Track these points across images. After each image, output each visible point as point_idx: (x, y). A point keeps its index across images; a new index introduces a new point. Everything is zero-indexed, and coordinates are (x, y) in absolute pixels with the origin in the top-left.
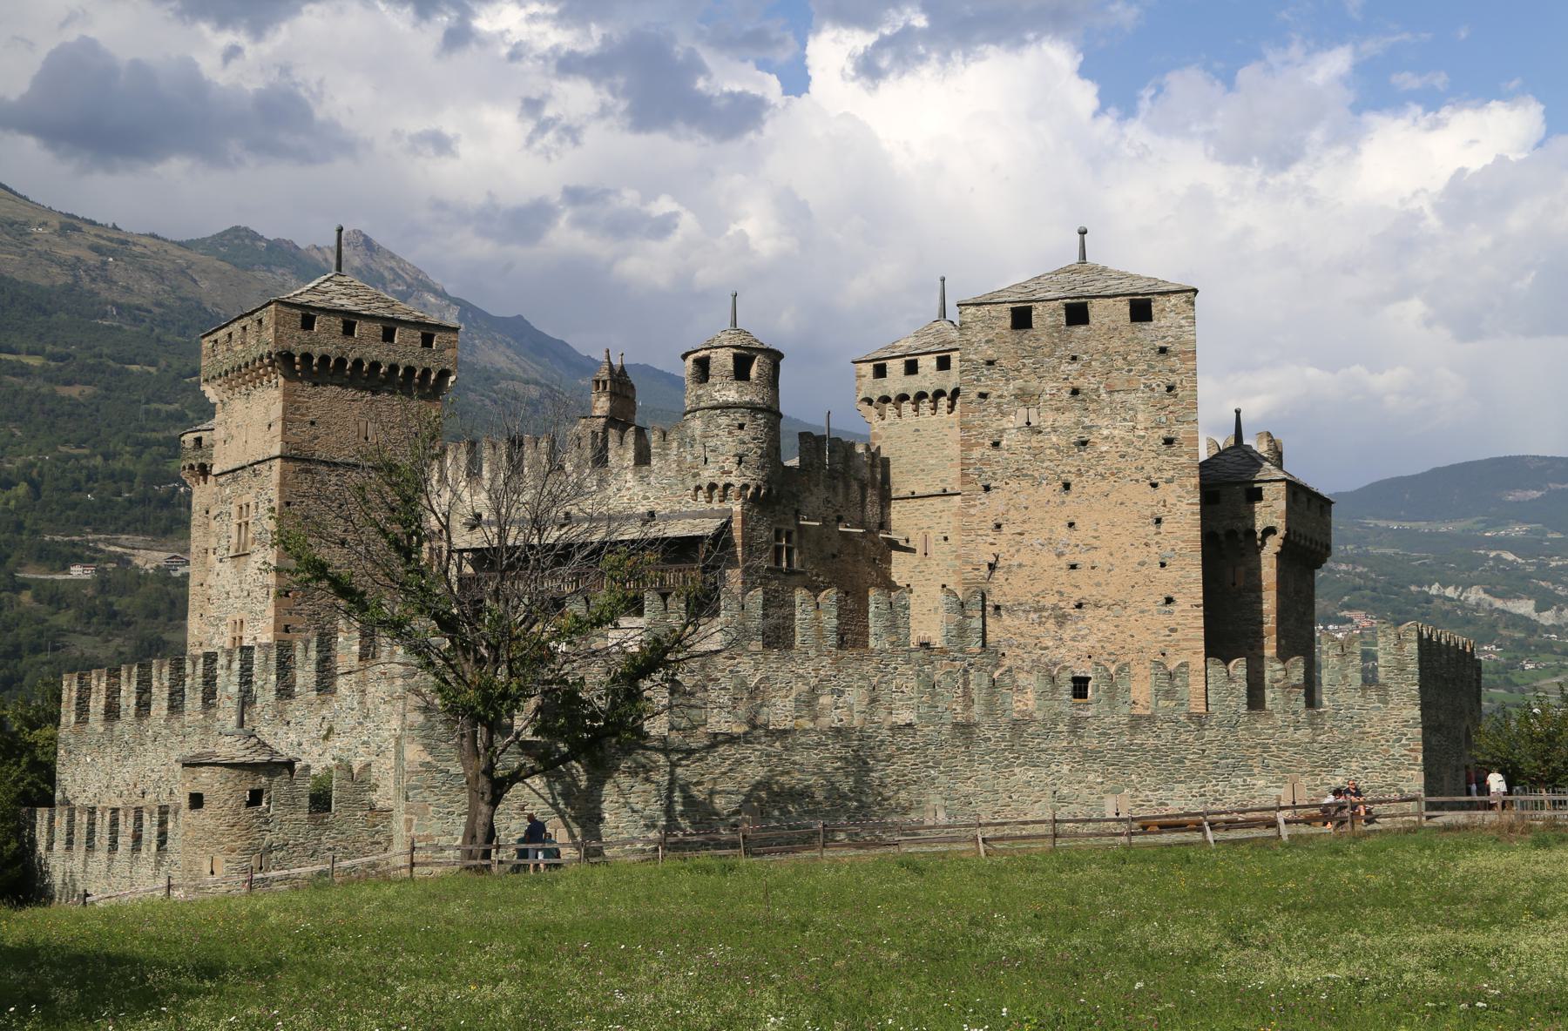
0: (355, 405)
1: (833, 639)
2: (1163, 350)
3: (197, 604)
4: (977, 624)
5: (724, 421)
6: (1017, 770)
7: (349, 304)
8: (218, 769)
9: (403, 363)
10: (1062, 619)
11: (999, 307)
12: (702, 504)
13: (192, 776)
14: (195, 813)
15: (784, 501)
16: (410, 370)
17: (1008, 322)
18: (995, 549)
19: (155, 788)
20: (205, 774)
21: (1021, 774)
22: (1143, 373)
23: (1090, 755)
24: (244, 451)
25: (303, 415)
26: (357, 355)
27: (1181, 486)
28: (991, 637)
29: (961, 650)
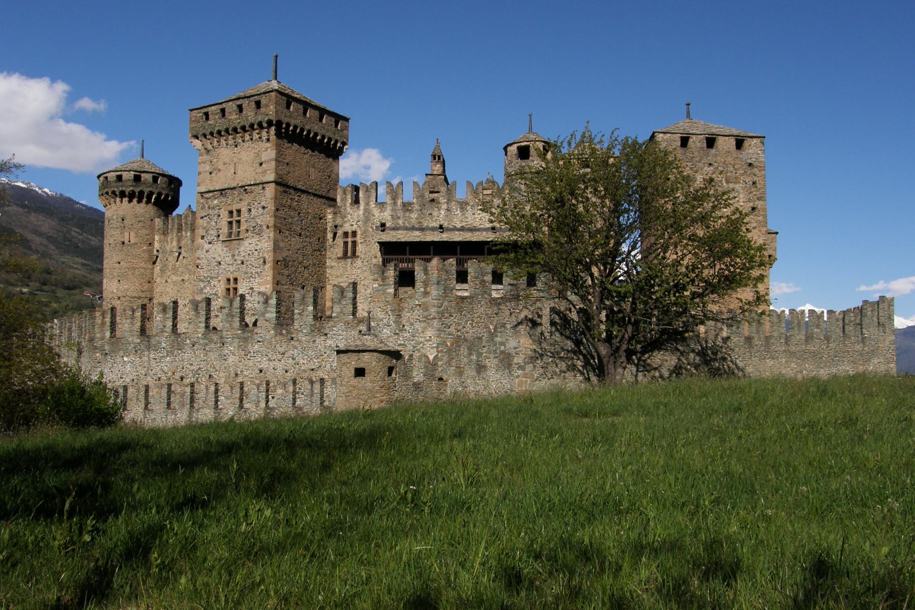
0: (305, 156)
2: (750, 165)
3: (115, 274)
6: (767, 361)
8: (375, 354)
9: (328, 134)
11: (675, 136)
13: (357, 358)
14: (359, 379)
17: (679, 144)
19: (194, 375)
20: (366, 356)
22: (742, 175)
24: (234, 179)
25: (284, 159)
26: (309, 128)
27: (760, 231)
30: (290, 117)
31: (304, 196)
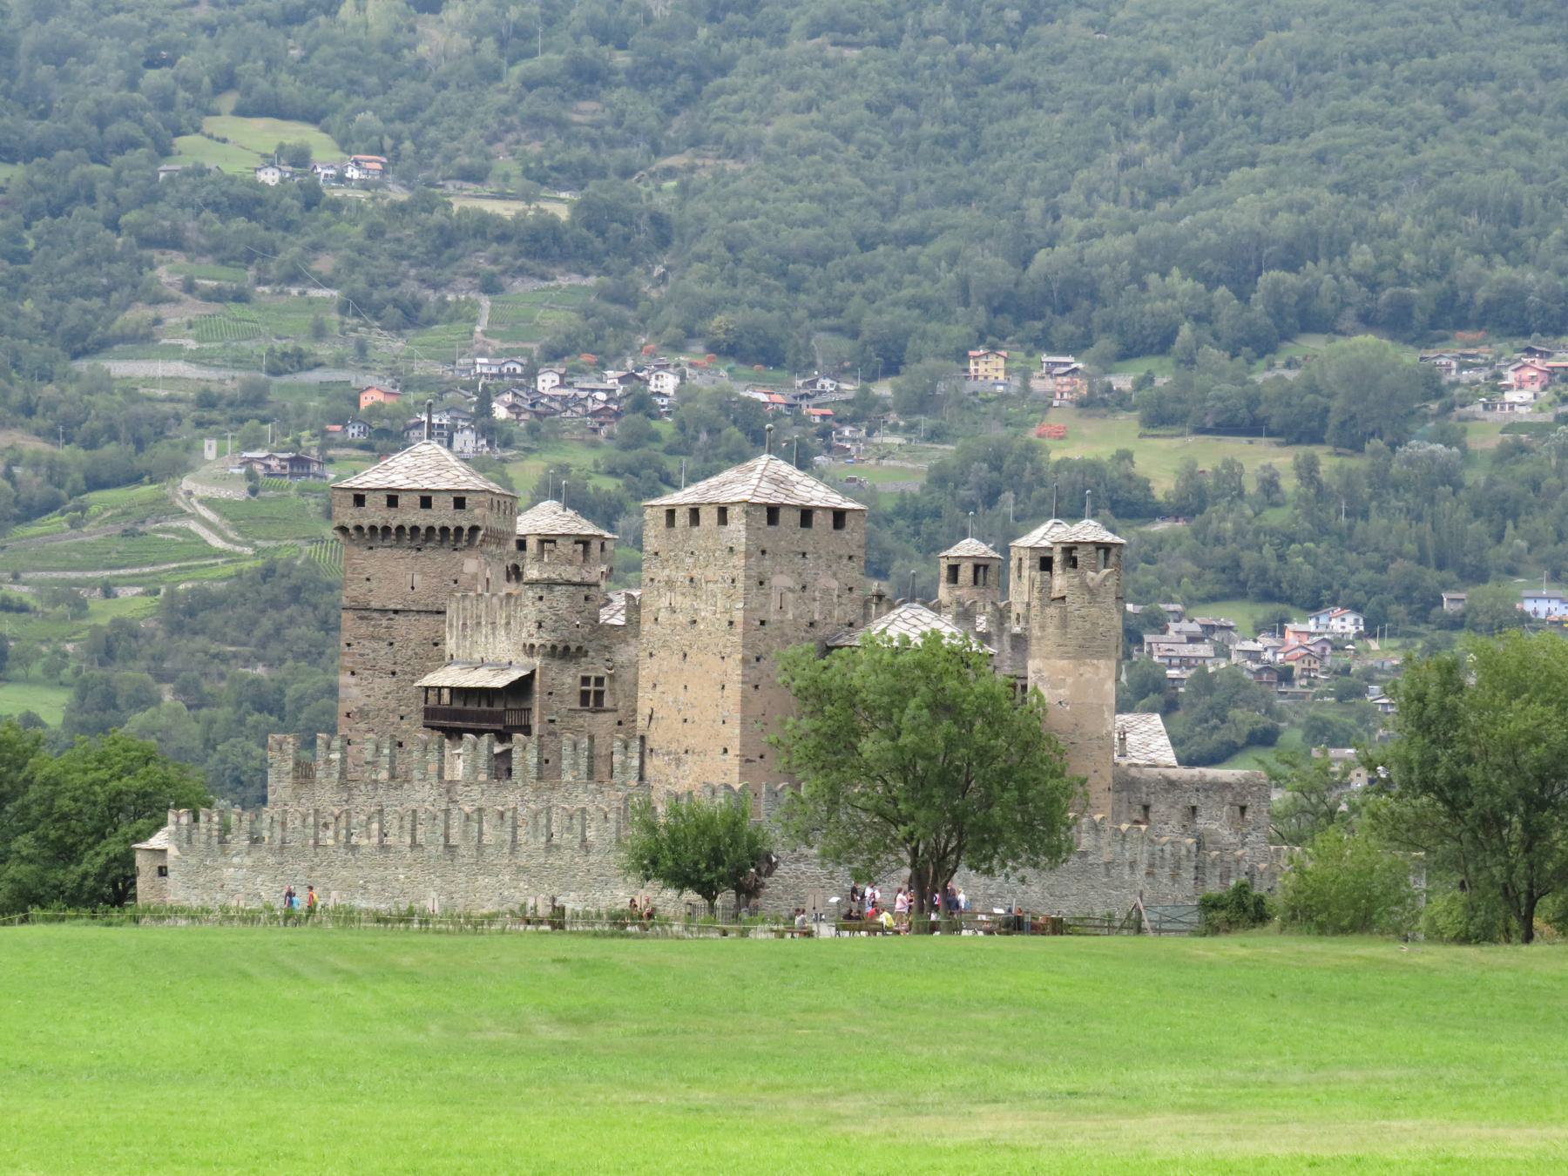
1: (534, 773)
2: (731, 549)
4: (636, 763)
5: (530, 594)
7: (399, 481)
9: (437, 525)
10: (678, 761)
12: (524, 659)
15: (591, 653)
16: (444, 530)
17: (664, 521)
18: (651, 704)
21: (483, 881)
23: (522, 870)
28: (649, 771)
29: (624, 783)
30: (362, 516)
31: (399, 618)
